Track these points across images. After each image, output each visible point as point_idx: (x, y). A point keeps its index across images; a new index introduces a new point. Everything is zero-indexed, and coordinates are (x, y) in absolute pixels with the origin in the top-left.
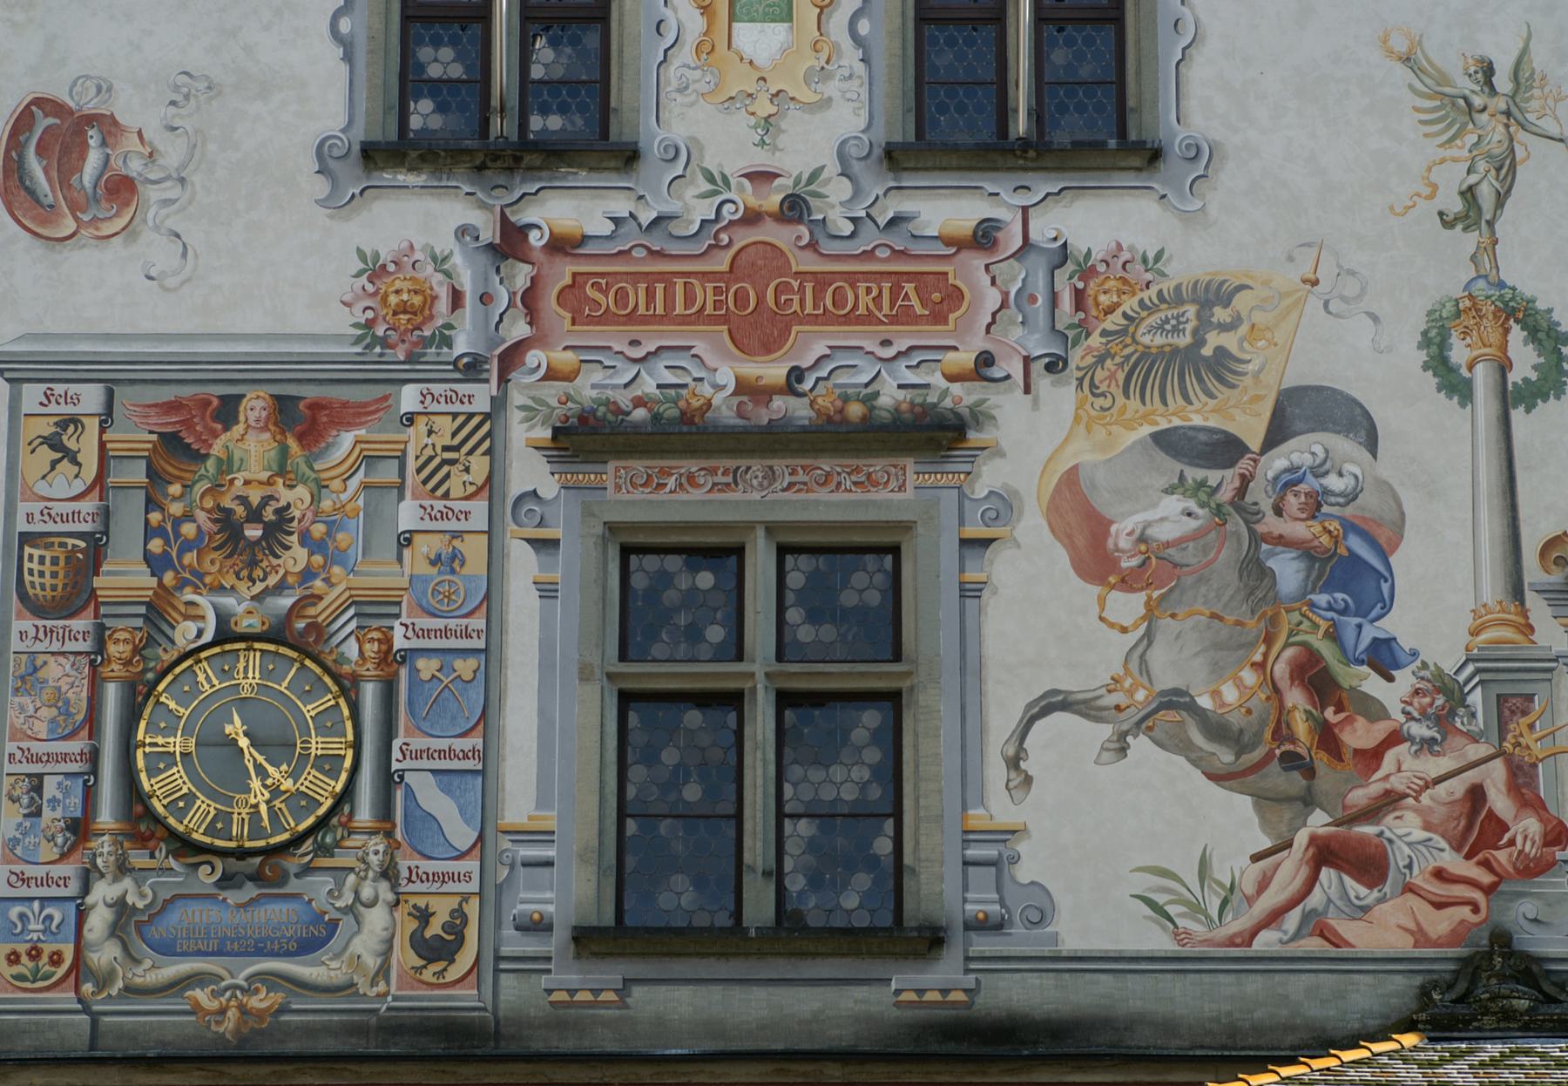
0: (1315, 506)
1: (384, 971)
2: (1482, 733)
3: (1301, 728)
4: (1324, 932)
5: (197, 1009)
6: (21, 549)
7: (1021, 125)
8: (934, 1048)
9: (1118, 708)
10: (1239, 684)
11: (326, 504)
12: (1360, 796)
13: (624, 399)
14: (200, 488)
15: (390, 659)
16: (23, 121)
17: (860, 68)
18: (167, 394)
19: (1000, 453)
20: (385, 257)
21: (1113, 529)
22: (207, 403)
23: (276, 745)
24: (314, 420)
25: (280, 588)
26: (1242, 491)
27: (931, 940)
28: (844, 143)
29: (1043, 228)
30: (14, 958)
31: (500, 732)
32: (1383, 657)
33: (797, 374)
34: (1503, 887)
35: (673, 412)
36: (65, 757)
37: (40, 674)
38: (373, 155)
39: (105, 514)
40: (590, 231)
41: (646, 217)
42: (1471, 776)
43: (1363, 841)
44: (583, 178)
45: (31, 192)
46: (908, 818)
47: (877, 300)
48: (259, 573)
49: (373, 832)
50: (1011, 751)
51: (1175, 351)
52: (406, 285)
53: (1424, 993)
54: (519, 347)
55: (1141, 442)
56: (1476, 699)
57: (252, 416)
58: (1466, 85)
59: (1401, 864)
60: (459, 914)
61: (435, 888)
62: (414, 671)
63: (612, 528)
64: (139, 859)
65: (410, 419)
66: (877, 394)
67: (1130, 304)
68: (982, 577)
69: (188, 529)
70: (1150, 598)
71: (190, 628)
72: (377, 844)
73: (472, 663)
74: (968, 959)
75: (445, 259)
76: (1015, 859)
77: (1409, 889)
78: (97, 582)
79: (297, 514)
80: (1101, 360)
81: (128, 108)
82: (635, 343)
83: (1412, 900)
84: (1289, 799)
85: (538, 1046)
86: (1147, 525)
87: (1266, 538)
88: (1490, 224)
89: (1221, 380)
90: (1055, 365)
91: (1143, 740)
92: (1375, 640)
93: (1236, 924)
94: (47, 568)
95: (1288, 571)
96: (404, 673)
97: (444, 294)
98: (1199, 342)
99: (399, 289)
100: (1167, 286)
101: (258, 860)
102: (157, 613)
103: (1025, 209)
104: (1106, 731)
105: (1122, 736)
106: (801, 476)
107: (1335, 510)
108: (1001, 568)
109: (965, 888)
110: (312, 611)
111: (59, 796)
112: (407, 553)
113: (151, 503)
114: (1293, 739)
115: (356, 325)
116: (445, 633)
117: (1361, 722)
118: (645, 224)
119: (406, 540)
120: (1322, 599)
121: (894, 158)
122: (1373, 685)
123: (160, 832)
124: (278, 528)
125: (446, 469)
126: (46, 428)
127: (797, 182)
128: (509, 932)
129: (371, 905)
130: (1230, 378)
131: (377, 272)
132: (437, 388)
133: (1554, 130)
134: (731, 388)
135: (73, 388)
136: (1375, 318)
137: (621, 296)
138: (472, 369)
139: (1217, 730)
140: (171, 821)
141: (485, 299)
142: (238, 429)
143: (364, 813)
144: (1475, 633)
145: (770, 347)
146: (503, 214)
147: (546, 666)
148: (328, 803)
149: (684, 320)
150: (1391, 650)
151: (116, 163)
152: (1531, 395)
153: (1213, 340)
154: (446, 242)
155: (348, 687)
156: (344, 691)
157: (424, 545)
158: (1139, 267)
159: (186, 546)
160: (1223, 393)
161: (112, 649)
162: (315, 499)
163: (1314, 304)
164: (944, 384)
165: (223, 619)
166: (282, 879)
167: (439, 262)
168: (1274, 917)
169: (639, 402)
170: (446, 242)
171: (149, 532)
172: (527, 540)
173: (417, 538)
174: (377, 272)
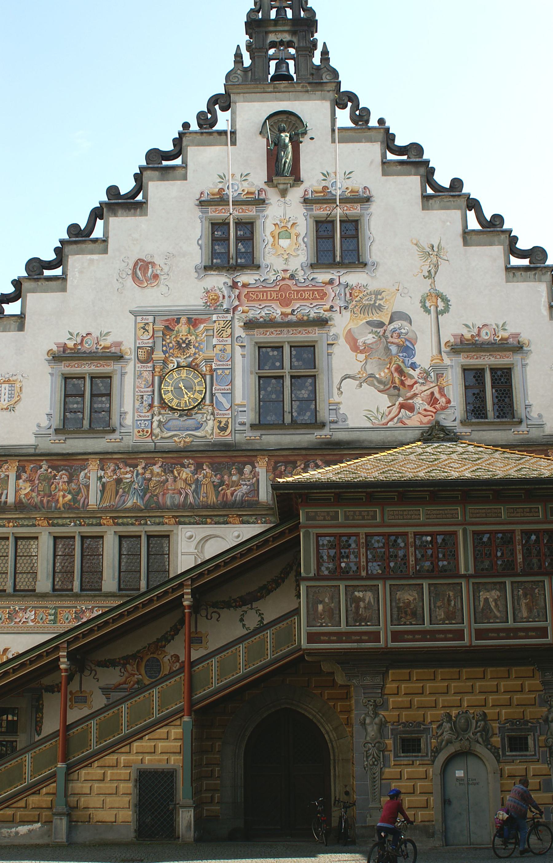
1: (212, 433)
3: (397, 381)
4: (402, 422)
5: (175, 441)
7: (338, 259)
8: (324, 447)
10: (384, 372)
11: (198, 339)
12: (409, 394)
13: (258, 317)
14: (173, 337)
15: (212, 371)
16: (136, 264)
17: (305, 248)
18: (166, 318)
19: (335, 326)
20: (209, 289)
23: (190, 388)
24: (195, 322)
25: (189, 357)
26: (384, 333)
27: (323, 425)
30: (139, 432)
32: (413, 366)
33: (293, 311)
35: (268, 319)
36: (148, 392)
38: (206, 268)
39: (154, 342)
40: (251, 283)
41: (262, 280)
43: (410, 403)
44: (249, 272)
45: (138, 278)
46: (317, 401)
48: (185, 354)
50: (338, 387)
51: (370, 304)
52: (213, 295)
53: (422, 434)
54: (237, 306)
56: (432, 374)
58: (428, 250)
60: (227, 421)
63: (256, 343)
64: (163, 412)
65: (215, 322)
67: (361, 295)
69: (171, 345)
71: (172, 365)
72: (210, 408)
73: (228, 371)
76: (339, 409)
77: (419, 413)
80: (355, 307)
81: (157, 260)
82: (260, 305)
85: (244, 448)
88: (434, 278)
89: (380, 310)
90: (346, 308)
93: (384, 421)
94: (143, 353)
95: (394, 349)
96: (215, 373)
98: (375, 303)
99: (212, 295)
100: (368, 291)
102: (165, 362)
104: (358, 382)
106: (294, 332)
108: (336, 350)
110: (196, 361)
113: (163, 340)
114: (395, 383)
116: (223, 365)
117: (409, 379)
119: (215, 346)
120: (401, 355)
121: (312, 266)
122: (411, 372)
123: (167, 406)
124: (189, 344)
128: (237, 425)
130: (382, 310)
131: (208, 292)
133: (446, 259)
135: (147, 317)
136: (411, 297)
137: (257, 296)
138: (227, 311)
139: (380, 382)
140: (169, 404)
141: (229, 297)
142: (180, 324)
143: (208, 402)
144: (432, 361)
145: (287, 305)
146: (233, 280)
149: (270, 300)
151: (155, 271)
152: (443, 312)
153: (378, 302)
154: (221, 286)
155: (204, 376)
156: (203, 377)
159: (170, 349)
161: (156, 370)
162: (196, 338)
163: (398, 295)
164: (323, 312)
165: (178, 363)
166: (191, 415)
167: (220, 289)
168: (392, 419)
169: (261, 317)
170: (221, 286)
171: (163, 346)
173: (217, 346)
174: (208, 292)
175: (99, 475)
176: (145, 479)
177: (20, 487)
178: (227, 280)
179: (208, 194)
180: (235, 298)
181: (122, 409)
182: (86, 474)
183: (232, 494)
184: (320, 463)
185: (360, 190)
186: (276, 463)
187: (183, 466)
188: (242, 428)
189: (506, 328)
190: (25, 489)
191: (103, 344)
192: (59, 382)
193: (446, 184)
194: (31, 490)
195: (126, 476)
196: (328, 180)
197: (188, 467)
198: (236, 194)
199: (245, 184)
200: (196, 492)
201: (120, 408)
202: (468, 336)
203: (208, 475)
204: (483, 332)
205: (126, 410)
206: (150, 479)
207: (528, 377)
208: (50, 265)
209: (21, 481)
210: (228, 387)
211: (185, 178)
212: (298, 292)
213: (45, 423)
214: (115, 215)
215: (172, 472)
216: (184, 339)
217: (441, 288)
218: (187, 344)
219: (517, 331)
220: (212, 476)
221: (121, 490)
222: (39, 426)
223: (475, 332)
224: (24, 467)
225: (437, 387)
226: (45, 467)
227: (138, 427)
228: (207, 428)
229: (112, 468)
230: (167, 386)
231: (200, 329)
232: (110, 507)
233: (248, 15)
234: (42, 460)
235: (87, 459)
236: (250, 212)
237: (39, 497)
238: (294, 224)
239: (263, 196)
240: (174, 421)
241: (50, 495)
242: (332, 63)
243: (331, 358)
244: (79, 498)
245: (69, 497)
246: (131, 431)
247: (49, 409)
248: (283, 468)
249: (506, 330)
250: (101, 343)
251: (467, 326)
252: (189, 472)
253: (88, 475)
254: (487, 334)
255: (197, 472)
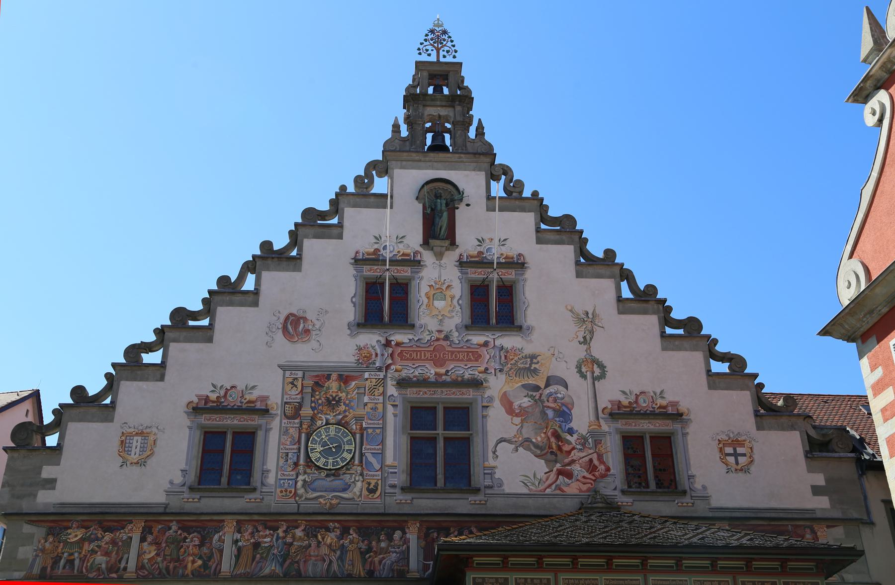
0: (555, 400)
1: (361, 495)
2: (591, 448)
3: (554, 446)
4: (560, 489)
5: (320, 503)
6: (285, 405)
9: (516, 441)
10: (541, 437)
11: (349, 397)
12: (567, 461)
13: (411, 376)
15: (362, 429)
16: (287, 318)
17: (460, 310)
18: (316, 374)
19: (490, 389)
21: (514, 404)
22: (324, 375)
25: (339, 414)
26: (540, 397)
28: (457, 325)
29: (498, 343)
30: (281, 492)
31: (386, 444)
32: (571, 432)
33: (447, 371)
34: (597, 480)
36: (293, 449)
37: (288, 431)
38: (359, 325)
41: (416, 339)
42: (590, 457)
45: (289, 332)
47: (464, 356)
49: (358, 466)
51: (526, 368)
54: (389, 365)
55: (519, 386)
56: (590, 440)
57: (334, 378)
59: (576, 475)
60: (377, 483)
61: (372, 478)
62: (367, 432)
64: (308, 471)
65: (367, 379)
66: (464, 376)
67: (516, 358)
68: (486, 414)
69: (320, 401)
70: (522, 419)
72: (359, 468)
73: (379, 430)
74: (485, 494)
75: (374, 347)
76: (495, 473)
77: (578, 480)
78: (300, 412)
79: (343, 399)
80: (511, 369)
82: (413, 364)
83: (578, 482)
84: (552, 461)
86: (521, 403)
87: (546, 406)
88: (589, 344)
89: (536, 374)
91: (521, 447)
92: (569, 428)
93: (541, 487)
94: (290, 409)
95: (550, 413)
96: (365, 432)
97: (374, 354)
98: (531, 365)
100: (524, 355)
101: (334, 471)
102: (313, 419)
103: (494, 339)
104: (513, 446)
105: (517, 447)
106: (448, 392)
107: (559, 401)
109: (484, 479)
110: (346, 419)
111: (292, 457)
112: (366, 407)
113: (312, 396)
114: (552, 449)
115: (355, 360)
116: (374, 424)
118: (416, 340)
119: (366, 404)
120: (558, 419)
121: (467, 327)
122: (569, 437)
123: (313, 465)
125: (374, 390)
126: (291, 380)
127: (447, 332)
128: (387, 487)
129: (358, 481)
130: (537, 374)
131: (360, 349)
132: (372, 373)
133: (601, 326)
134: (434, 374)
135: (296, 372)
137: (411, 355)
139: (537, 446)
141: (383, 355)
143: (357, 462)
144: (589, 427)
145: (441, 366)
147: (395, 431)
148: (349, 459)
149: (424, 360)
150: (572, 430)
151: (306, 326)
152: (599, 378)
154: (374, 343)
155: (354, 435)
157: (369, 406)
158: (518, 351)
159: (319, 405)
160: (536, 377)
161: (304, 426)
163: (554, 359)
164: (478, 374)
165: (327, 420)
166: (339, 475)
167: (373, 347)
168: (550, 486)
169: (414, 377)
170: (374, 343)
172: (391, 405)
173: (368, 404)
174: (360, 349)
175: (235, 538)
176: (285, 543)
177: (143, 550)
178: (380, 338)
179: (363, 254)
180: (388, 356)
181: (265, 467)
182: (220, 537)
183: (380, 562)
184: (474, 530)
185: (515, 256)
186: (428, 529)
187: (328, 530)
188: (392, 491)
189: (664, 396)
190: (150, 553)
191: (248, 397)
192: (198, 436)
193: (600, 254)
194: (155, 554)
195: (265, 540)
196: (484, 246)
197: (333, 531)
198: (391, 255)
199: (401, 246)
200: (341, 558)
201: (263, 466)
202: (625, 402)
203: (355, 540)
204: (641, 400)
205: (269, 468)
206: (291, 544)
207: (689, 447)
208: (195, 316)
209: (145, 544)
210: (378, 447)
211: (340, 237)
212: (452, 352)
213: (178, 479)
214: (268, 269)
215: (316, 536)
216: (334, 395)
217: (596, 354)
218: (336, 401)
219: (676, 399)
220: (359, 542)
221: (258, 556)
222: (171, 483)
223: (632, 399)
224: (150, 528)
225: (595, 454)
226: (174, 527)
227: (281, 486)
228: (355, 490)
229: (250, 531)
230: (314, 444)
231: (352, 386)
232: (244, 574)
233: (407, 89)
234: (171, 521)
235: (223, 521)
236: (405, 272)
237: (165, 562)
238: (449, 286)
239: (418, 258)
240: (321, 481)
241: (178, 560)
242: (487, 137)
243: (486, 421)
244: (210, 563)
245: (200, 562)
246: (273, 490)
247: (184, 464)
248: (435, 535)
249: (664, 398)
250: (245, 397)
251: (624, 392)
252: (334, 537)
253: (223, 537)
254: (645, 402)
255: (343, 537)
